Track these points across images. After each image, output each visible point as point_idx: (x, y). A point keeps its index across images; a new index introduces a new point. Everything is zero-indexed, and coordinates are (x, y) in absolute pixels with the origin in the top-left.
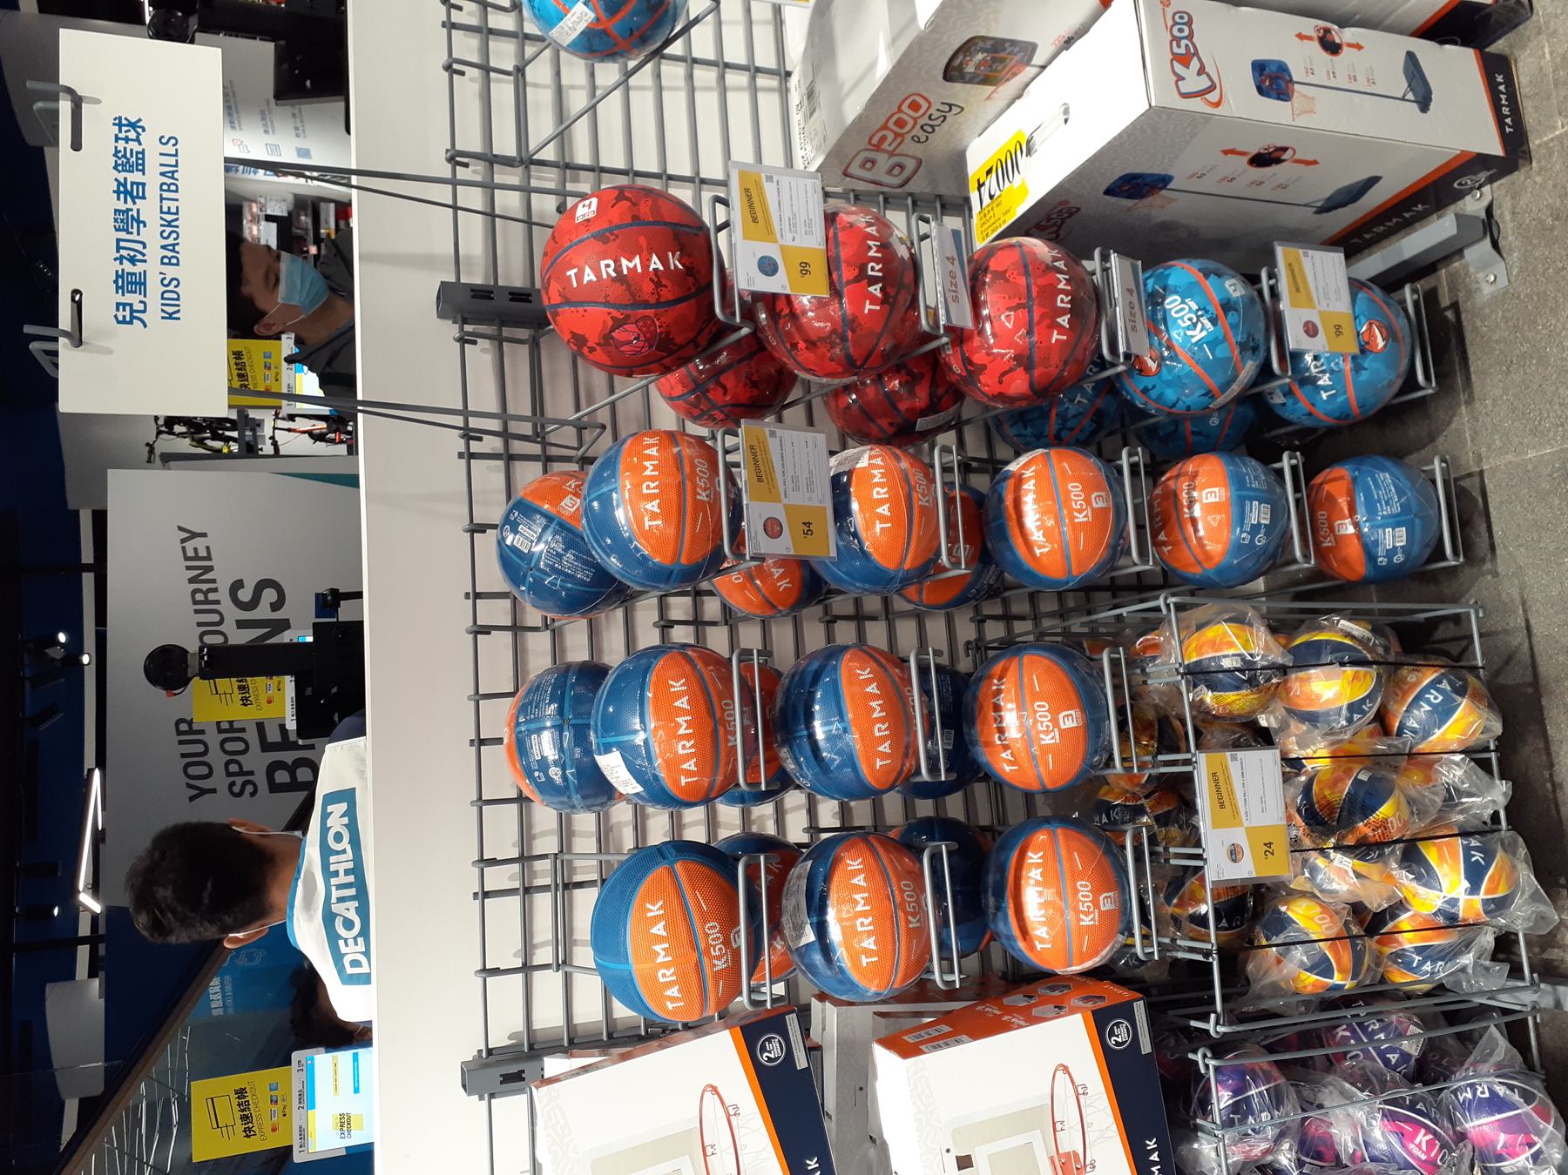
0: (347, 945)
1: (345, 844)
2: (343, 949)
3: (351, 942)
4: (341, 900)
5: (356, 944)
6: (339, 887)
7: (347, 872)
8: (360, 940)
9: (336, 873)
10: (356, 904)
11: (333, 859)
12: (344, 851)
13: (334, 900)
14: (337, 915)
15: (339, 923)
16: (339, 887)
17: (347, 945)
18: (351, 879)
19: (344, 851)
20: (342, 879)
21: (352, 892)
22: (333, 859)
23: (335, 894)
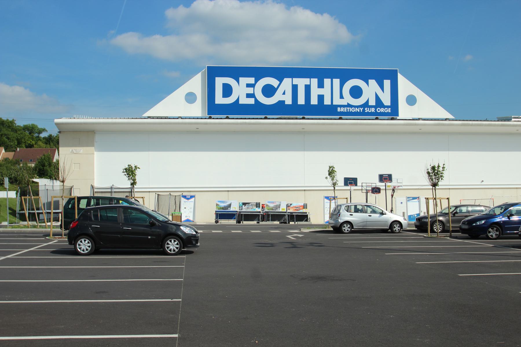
0: (248, 85)
1: (348, 99)
2: (244, 80)
3: (250, 90)
4: (295, 88)
5: (249, 96)
6: (308, 88)
7: (321, 98)
8: (251, 101)
9: (321, 85)
10: (289, 101)
11: (337, 82)
12: (342, 97)
13: (297, 81)
14: (281, 81)
15: (274, 82)
16: (308, 88)
17: (248, 85)
18: (314, 101)
19: (342, 97)
20: (315, 92)
21: (301, 101)
22: (337, 82)
23: (301, 82)
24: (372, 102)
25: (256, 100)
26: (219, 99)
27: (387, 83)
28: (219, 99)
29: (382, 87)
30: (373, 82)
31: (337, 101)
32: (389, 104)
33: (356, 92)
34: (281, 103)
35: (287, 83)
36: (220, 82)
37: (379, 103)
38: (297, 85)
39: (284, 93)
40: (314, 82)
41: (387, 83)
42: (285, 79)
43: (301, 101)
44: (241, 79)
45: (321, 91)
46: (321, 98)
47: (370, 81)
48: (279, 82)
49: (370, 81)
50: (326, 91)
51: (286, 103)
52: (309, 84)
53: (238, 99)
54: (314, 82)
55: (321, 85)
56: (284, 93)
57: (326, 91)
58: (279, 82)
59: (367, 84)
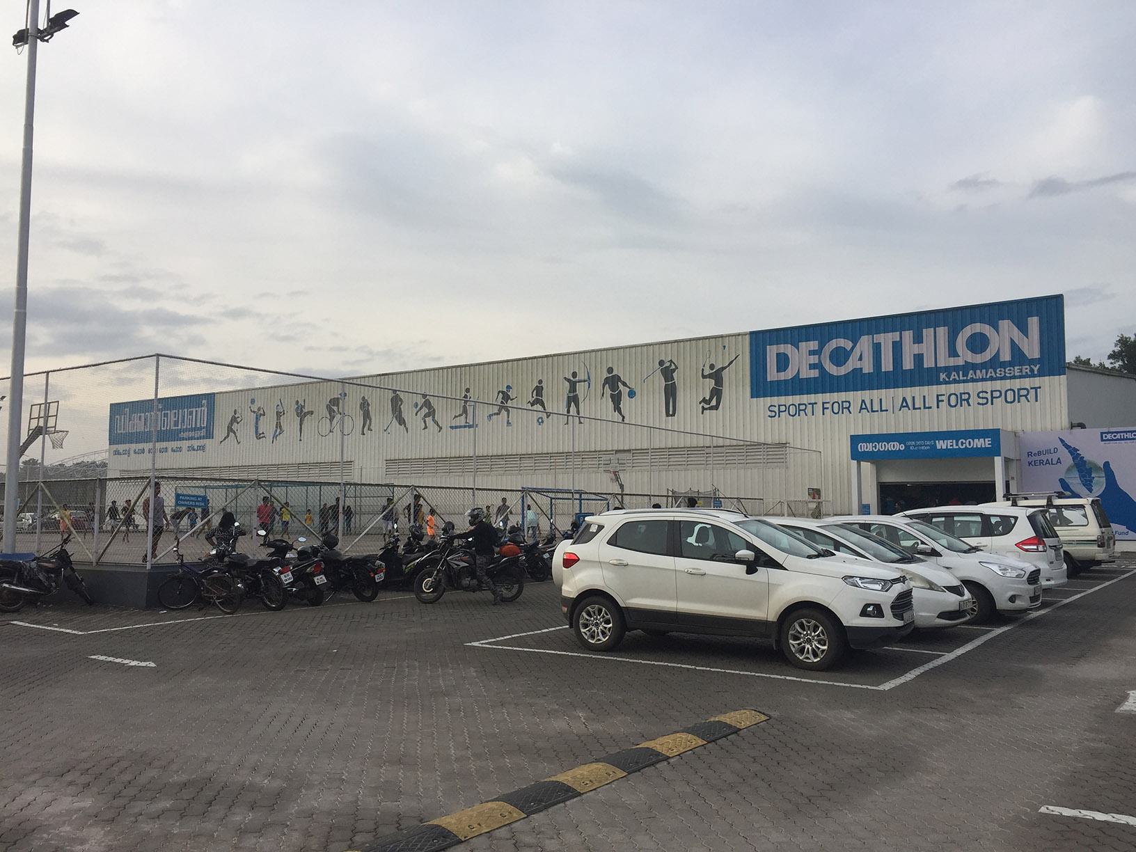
0: (812, 353)
3: (814, 359)
4: (877, 348)
5: (812, 366)
6: (897, 347)
7: (919, 358)
8: (814, 373)
9: (918, 339)
10: (868, 367)
11: (942, 332)
12: (953, 353)
15: (845, 343)
16: (897, 347)
17: (812, 353)
18: (908, 364)
21: (887, 365)
22: (942, 332)
23: (886, 340)
24: (1006, 356)
25: (822, 370)
26: (773, 375)
27: (1034, 322)
28: (773, 375)
29: (1024, 329)
30: (1005, 325)
32: (1037, 355)
33: (978, 343)
34: (857, 372)
35: (865, 343)
36: (772, 351)
37: (1018, 356)
39: (860, 359)
40: (908, 336)
41: (1034, 322)
45: (916, 349)
46: (919, 358)
50: (926, 348)
54: (908, 336)
55: (918, 339)
56: (860, 359)
57: (926, 348)
59: (996, 328)
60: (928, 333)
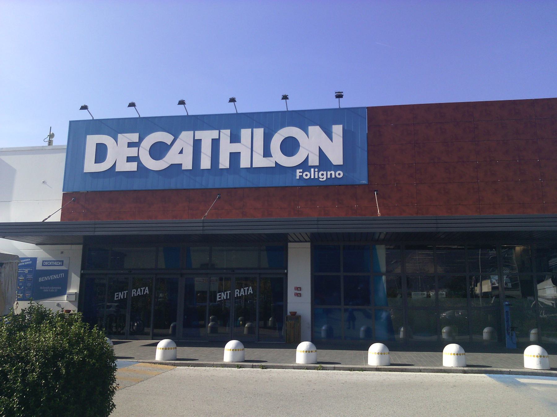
0: (130, 145)
3: (133, 152)
4: (197, 144)
5: (130, 159)
7: (235, 157)
9: (235, 138)
10: (188, 165)
11: (259, 133)
12: (267, 153)
13: (199, 134)
15: (165, 137)
16: (215, 143)
17: (130, 145)
19: (267, 153)
21: (206, 163)
24: (314, 161)
25: (140, 165)
27: (338, 130)
30: (315, 130)
31: (260, 162)
35: (186, 137)
36: (92, 141)
38: (200, 140)
39: (181, 152)
42: (183, 132)
43: (206, 163)
44: (120, 136)
45: (235, 148)
46: (235, 157)
47: (311, 129)
48: (172, 138)
49: (311, 129)
50: (242, 148)
51: (184, 168)
52: (218, 138)
53: (115, 164)
54: (226, 134)
55: (235, 138)
57: (242, 148)
58: (172, 138)
60: (245, 133)
